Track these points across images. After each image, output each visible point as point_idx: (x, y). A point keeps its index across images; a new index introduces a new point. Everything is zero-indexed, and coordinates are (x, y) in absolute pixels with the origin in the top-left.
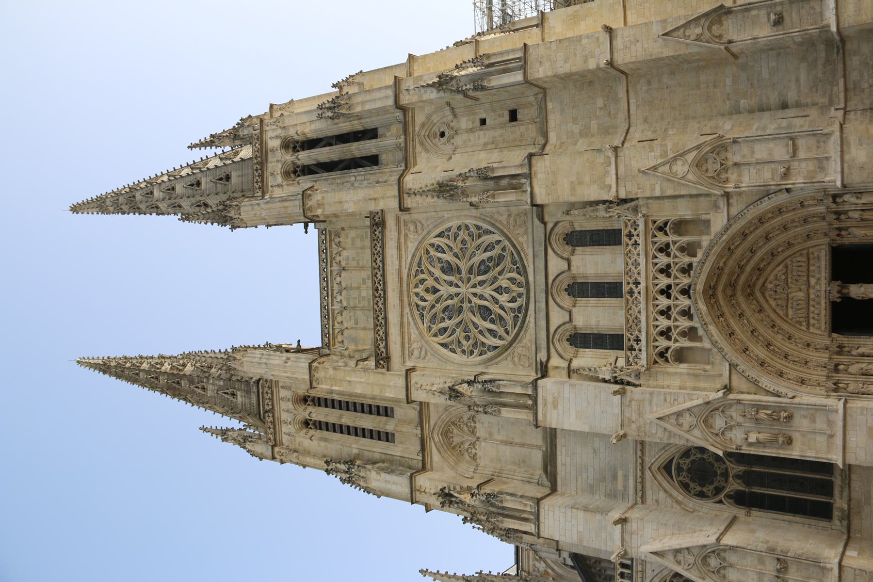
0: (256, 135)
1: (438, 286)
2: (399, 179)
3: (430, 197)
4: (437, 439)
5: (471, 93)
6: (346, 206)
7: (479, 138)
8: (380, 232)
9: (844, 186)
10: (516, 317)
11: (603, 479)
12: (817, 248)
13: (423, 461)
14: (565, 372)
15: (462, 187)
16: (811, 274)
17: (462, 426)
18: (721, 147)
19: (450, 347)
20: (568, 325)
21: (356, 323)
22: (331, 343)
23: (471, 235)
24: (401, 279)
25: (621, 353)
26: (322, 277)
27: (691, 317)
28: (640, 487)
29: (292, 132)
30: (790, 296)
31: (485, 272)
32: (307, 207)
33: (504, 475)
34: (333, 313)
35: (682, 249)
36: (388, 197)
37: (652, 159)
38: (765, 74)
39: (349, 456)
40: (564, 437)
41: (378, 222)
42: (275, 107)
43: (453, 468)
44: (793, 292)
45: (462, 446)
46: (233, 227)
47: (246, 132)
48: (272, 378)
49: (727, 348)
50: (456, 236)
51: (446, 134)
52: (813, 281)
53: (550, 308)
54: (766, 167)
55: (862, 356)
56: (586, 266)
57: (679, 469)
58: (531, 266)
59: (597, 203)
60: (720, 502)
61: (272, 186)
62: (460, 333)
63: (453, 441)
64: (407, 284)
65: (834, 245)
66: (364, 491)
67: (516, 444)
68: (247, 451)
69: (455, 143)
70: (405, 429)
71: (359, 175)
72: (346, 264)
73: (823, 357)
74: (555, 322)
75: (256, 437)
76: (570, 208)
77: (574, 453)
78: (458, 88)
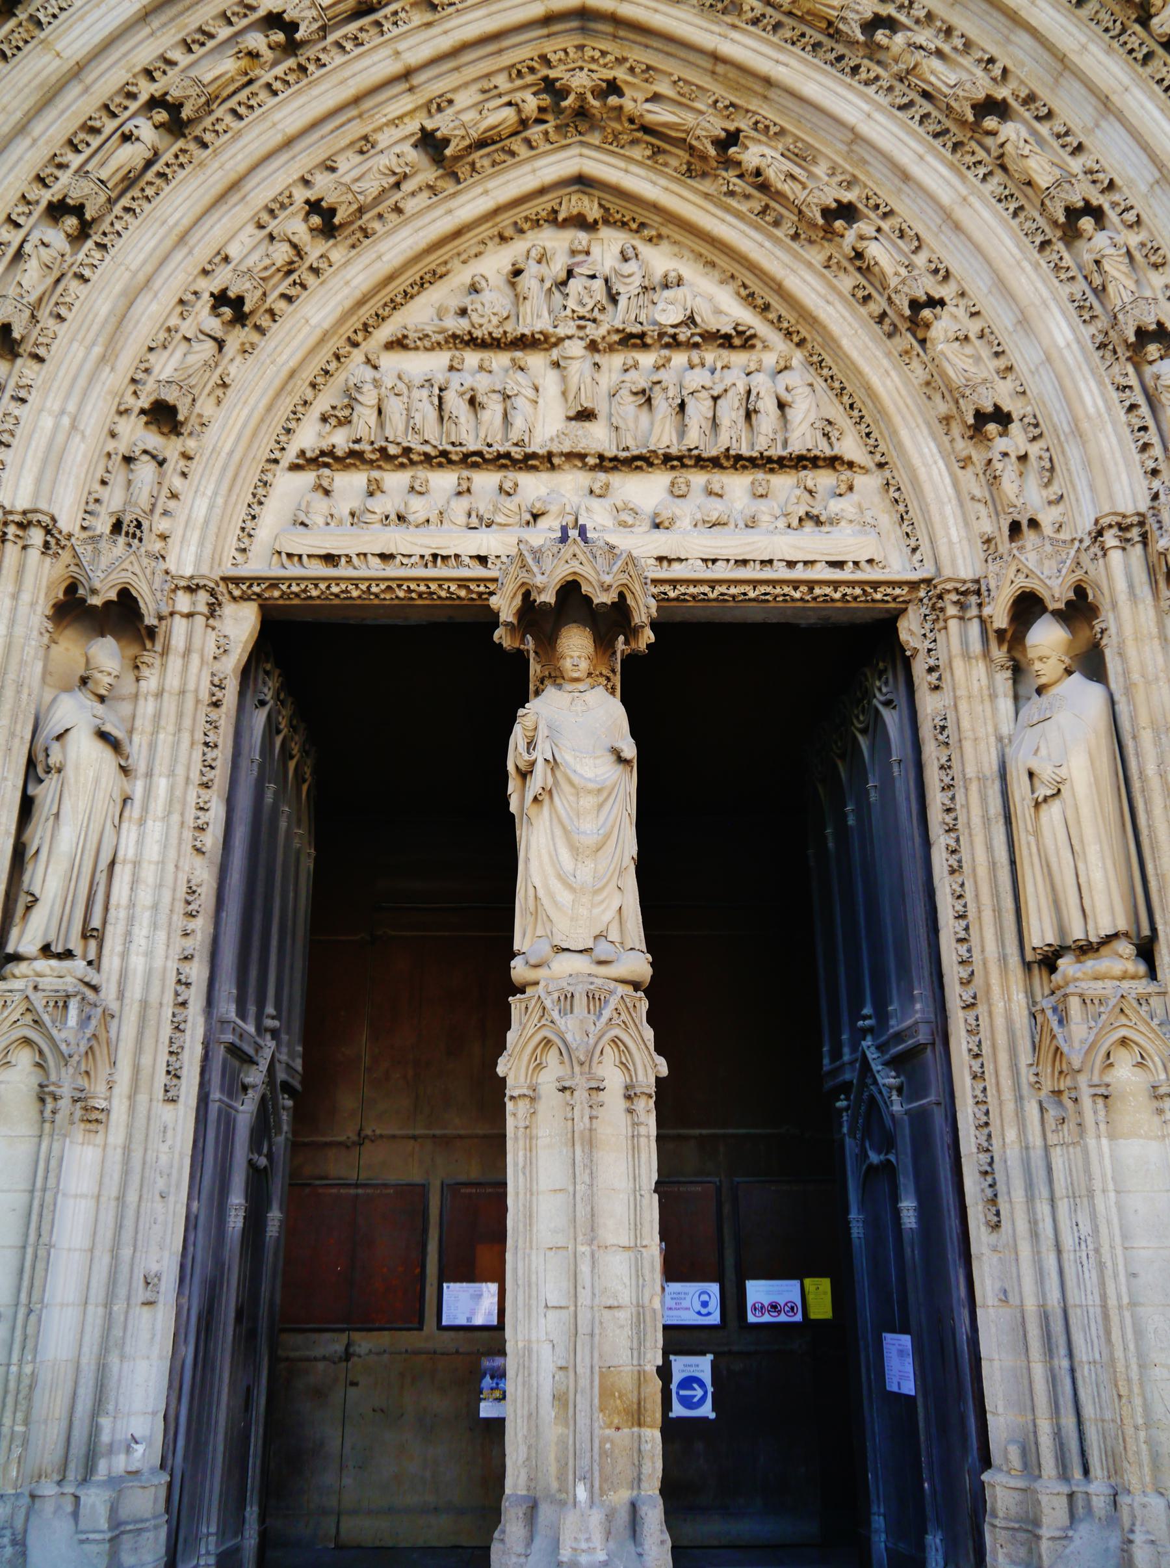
12: (886, 520)
16: (698, 479)
30: (536, 361)
44: (564, 379)
55: (31, 763)
65: (910, 630)
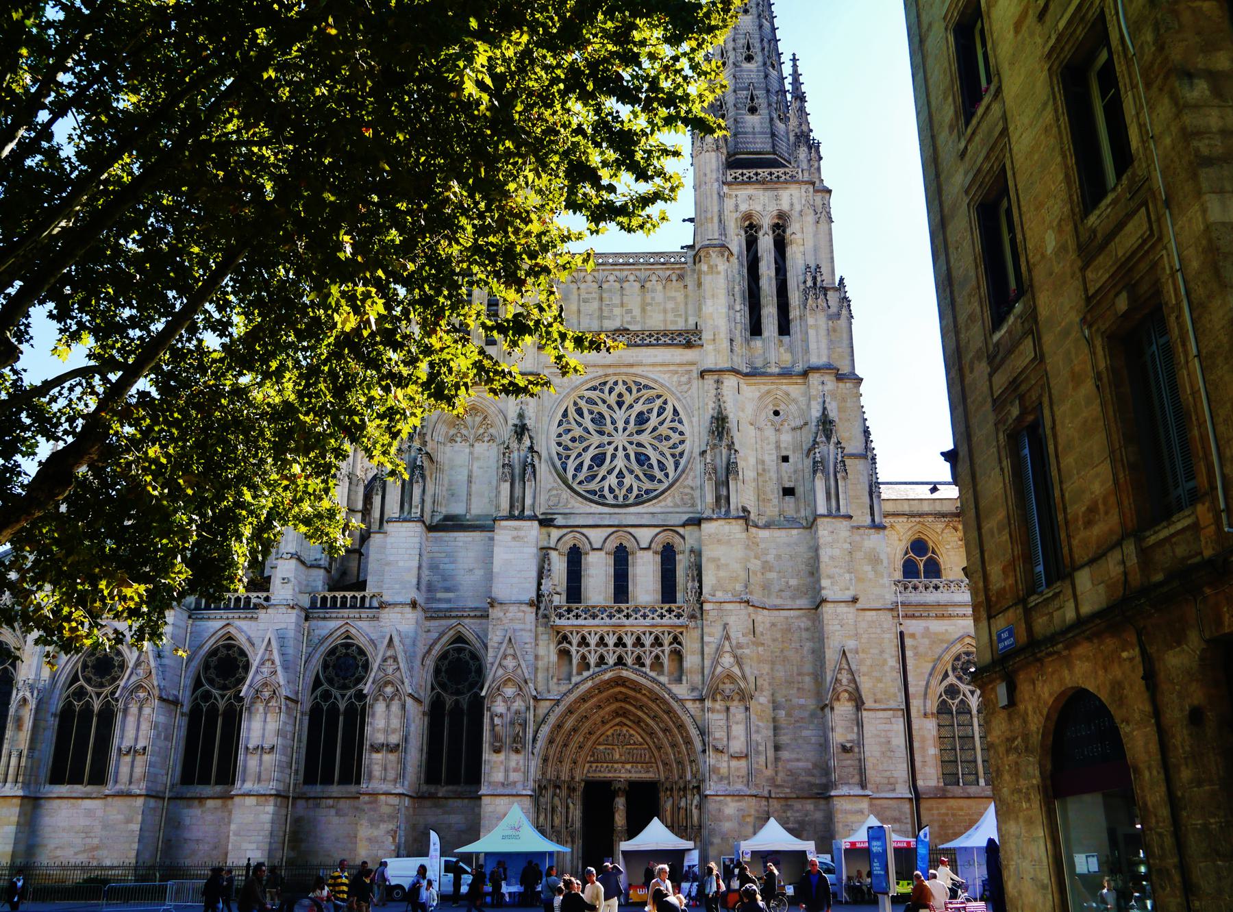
6: (709, 302)
9: (706, 796)
10: (594, 492)
11: (445, 580)
14: (546, 544)
18: (744, 697)
23: (674, 446)
24: (632, 365)
25: (564, 597)
27: (598, 665)
28: (441, 614)
29: (794, 228)
31: (638, 461)
35: (657, 657)
37: (737, 634)
38: (806, 733)
41: (689, 339)
49: (572, 697)
50: (674, 429)
52: (628, 766)
54: (725, 734)
57: (460, 650)
59: (700, 581)
60: (433, 688)
62: (578, 431)
67: (469, 487)
73: (565, 776)
76: (697, 553)
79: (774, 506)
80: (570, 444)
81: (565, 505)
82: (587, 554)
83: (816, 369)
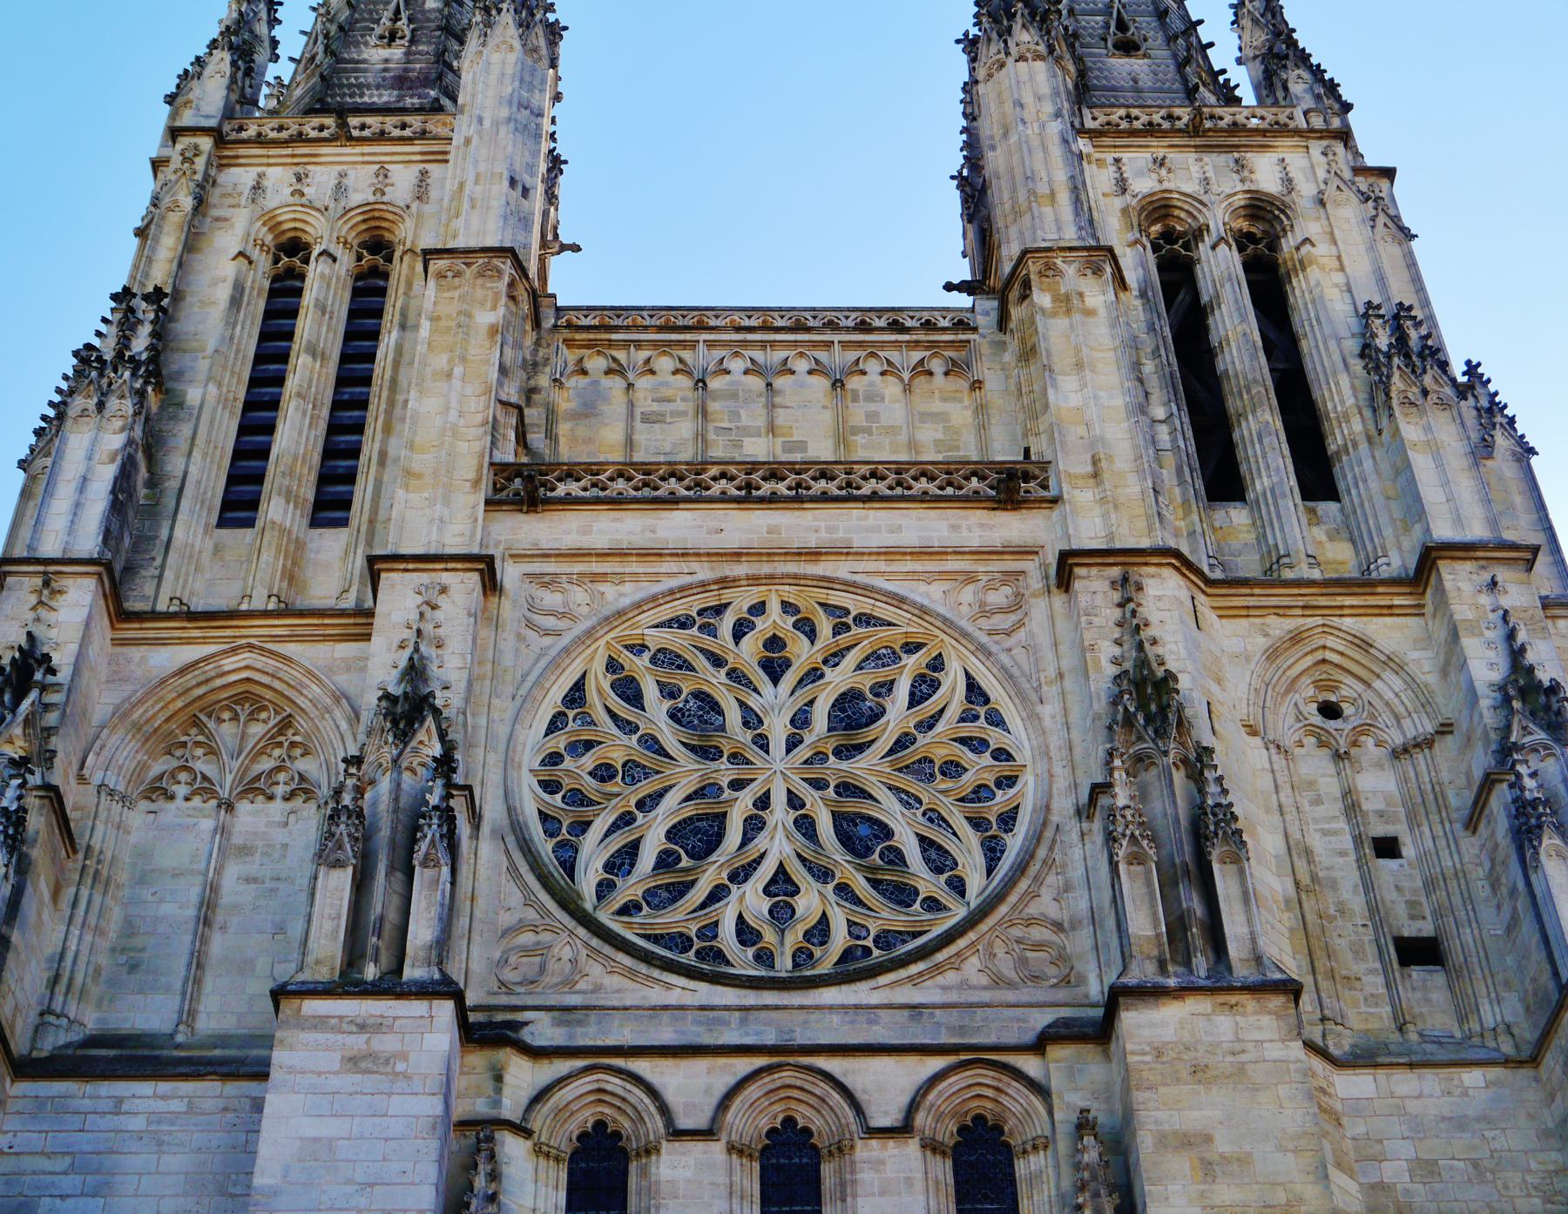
0: (1291, 118)
1: (790, 679)
2: (1177, 554)
3: (1117, 651)
4: (229, 663)
5: (1501, 796)
7: (1325, 833)
8: (976, 492)
10: (683, 943)
13: (154, 616)
14: (481, 1108)
15: (1166, 753)
17: (277, 752)
19: (571, 714)
20: (660, 1124)
21: (647, 419)
22: (578, 336)
23: (980, 793)
24: (814, 554)
26: (808, 315)
31: (846, 839)
32: (1059, 261)
33: (85, 893)
34: (682, 344)
36: (1105, 516)
39: (180, 374)
40: (225, 1109)
42: (1384, 184)
43: (121, 714)
45: (199, 752)
46: (970, 45)
47: (1297, 88)
48: (457, 140)
50: (976, 745)
51: (1331, 725)
53: (721, 1061)
56: (882, 1193)
58: (876, 998)
61: (1117, 161)
63: (220, 721)
64: (796, 576)
66: (44, 418)
67: (204, 941)
68: (198, 59)
69: (1301, 751)
70: (270, 562)
71: (1173, 432)
72: (855, 393)
74: (672, 1078)
75: (248, 90)
77: (160, 1143)
78: (1517, 747)
79: (1372, 999)
80: (590, 785)
81: (569, 983)
82: (650, 1150)
83: (1462, 550)
